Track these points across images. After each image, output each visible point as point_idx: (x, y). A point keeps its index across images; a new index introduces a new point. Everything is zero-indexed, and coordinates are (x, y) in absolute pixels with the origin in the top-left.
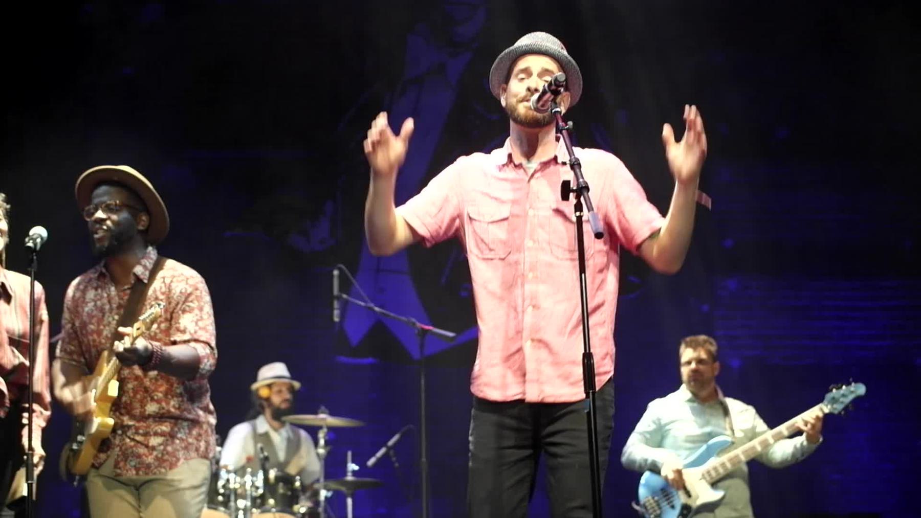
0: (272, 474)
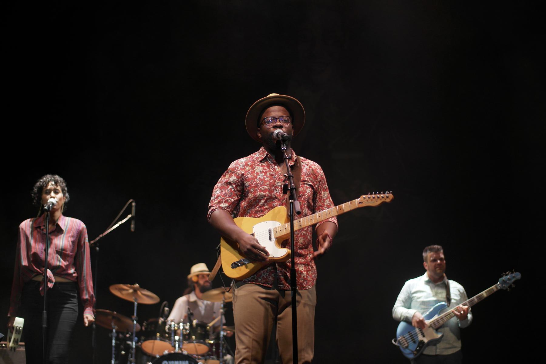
0: (195, 322)
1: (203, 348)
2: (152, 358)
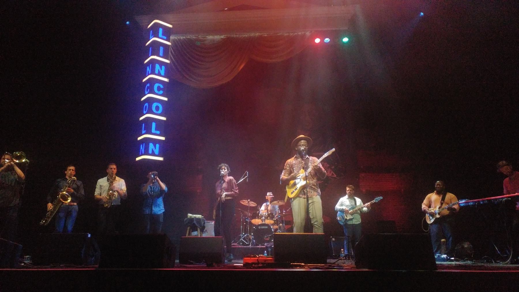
1: (272, 222)
2: (255, 225)
